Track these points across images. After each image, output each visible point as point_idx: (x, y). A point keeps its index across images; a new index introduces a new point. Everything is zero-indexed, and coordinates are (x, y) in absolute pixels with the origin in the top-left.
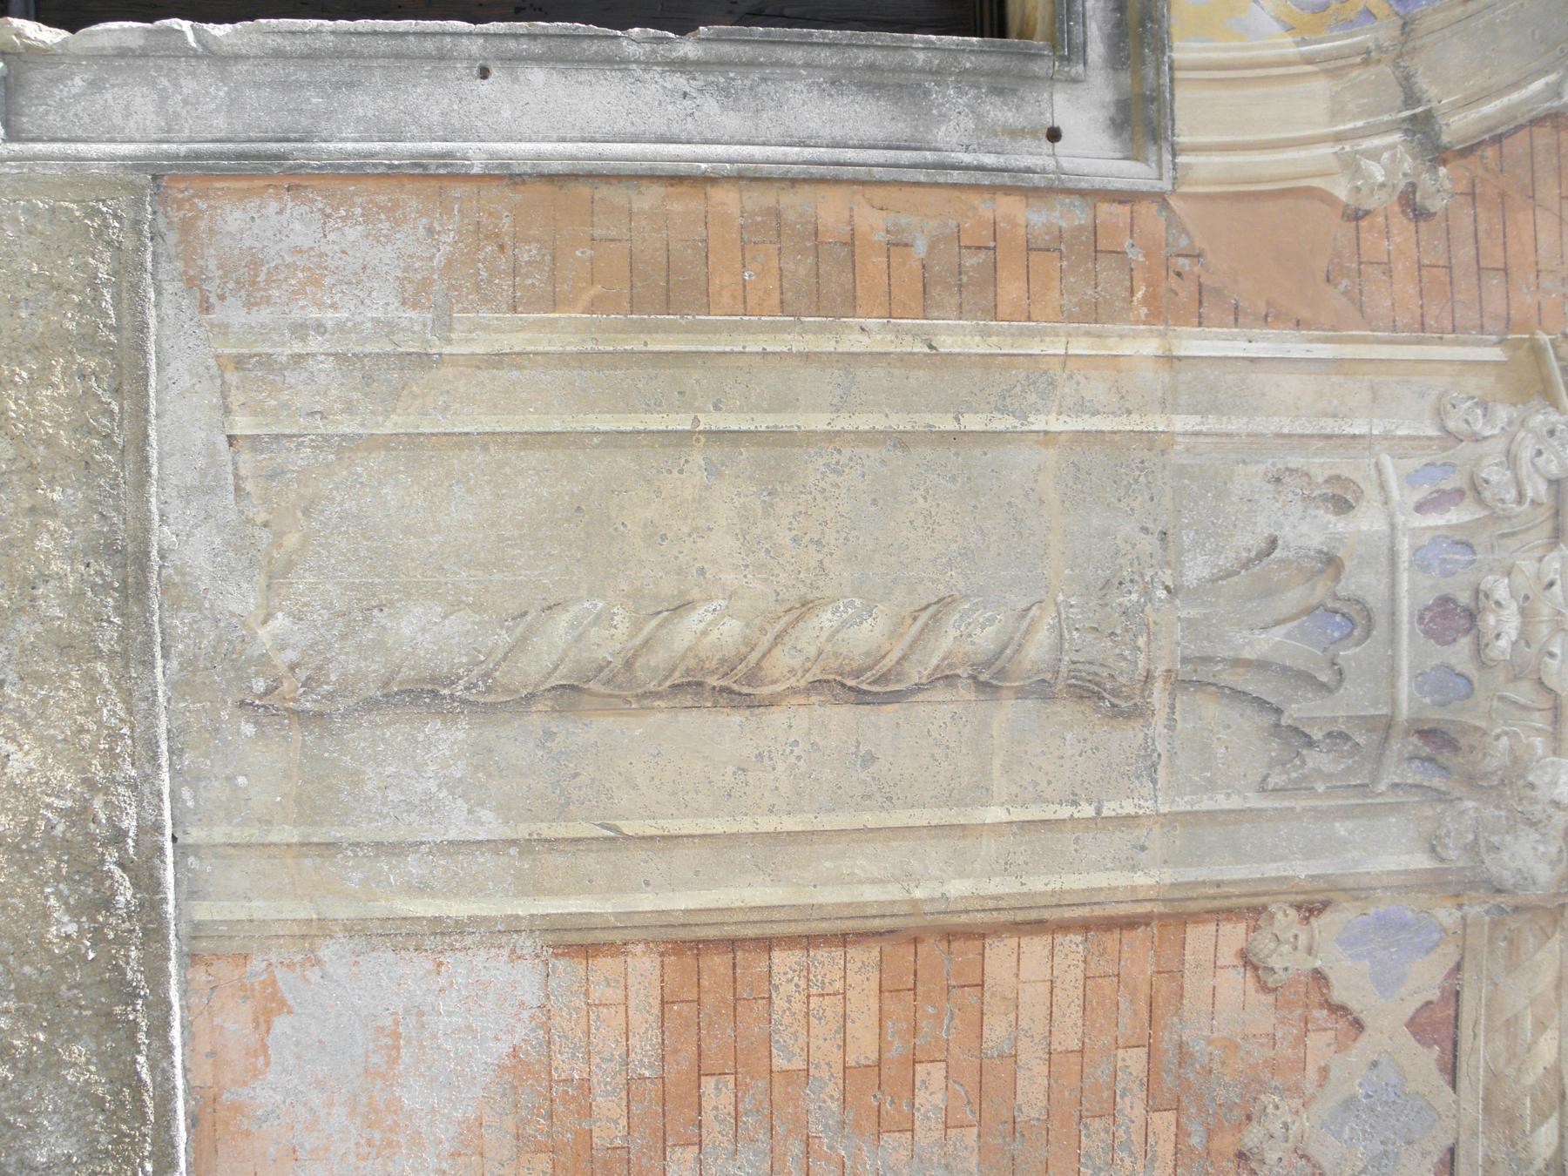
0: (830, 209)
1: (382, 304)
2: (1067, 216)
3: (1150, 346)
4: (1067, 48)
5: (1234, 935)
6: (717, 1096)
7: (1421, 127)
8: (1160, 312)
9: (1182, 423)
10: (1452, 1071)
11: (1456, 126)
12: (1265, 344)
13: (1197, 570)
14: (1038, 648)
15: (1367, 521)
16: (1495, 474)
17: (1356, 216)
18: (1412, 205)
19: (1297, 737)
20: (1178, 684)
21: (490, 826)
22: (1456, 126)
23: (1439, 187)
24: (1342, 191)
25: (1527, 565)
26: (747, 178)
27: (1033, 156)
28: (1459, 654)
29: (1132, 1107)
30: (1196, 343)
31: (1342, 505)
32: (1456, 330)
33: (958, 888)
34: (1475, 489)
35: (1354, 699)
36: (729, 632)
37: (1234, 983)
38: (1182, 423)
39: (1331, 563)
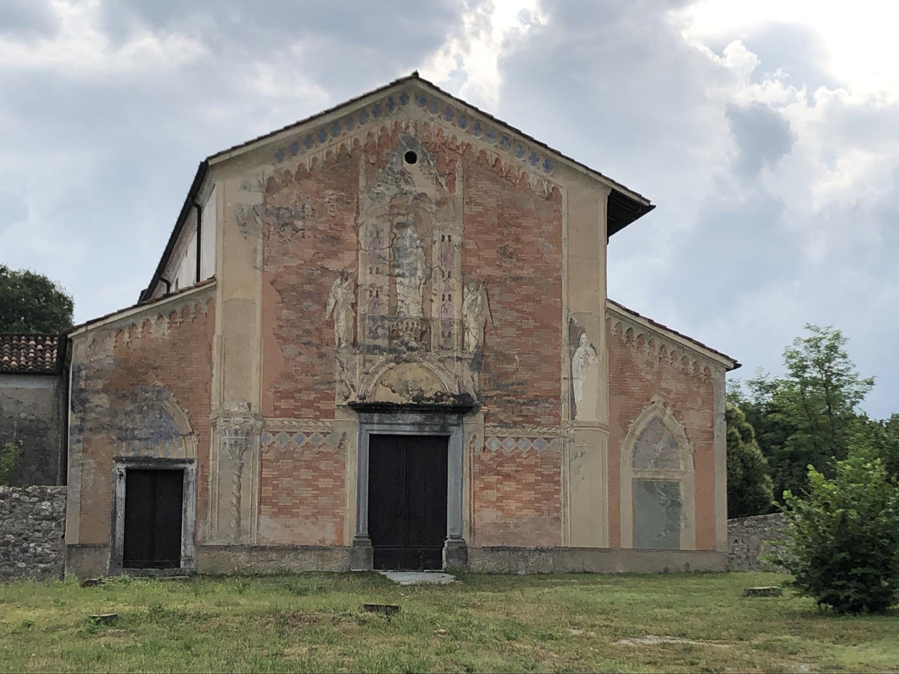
0: (199, 490)
1: (206, 526)
2: (200, 469)
3: (211, 462)
4: (185, 468)
5: (264, 454)
6: (274, 501)
7: (191, 434)
8: (208, 461)
9: (218, 459)
10: (278, 432)
11: (191, 430)
12: (211, 452)
13: (231, 458)
14: (237, 472)
15: (227, 441)
16: (223, 428)
17: (199, 442)
18: (198, 436)
19: (247, 448)
20: (241, 460)
21: (249, 519)
22: (191, 430)
23: (197, 432)
24: (197, 443)
25: (232, 425)
26: (197, 497)
27: (194, 472)
28: (239, 432)
29: (278, 464)
30: (211, 457)
31: (225, 443)
32: (210, 432)
33: (257, 479)
34: (224, 430)
35: (243, 442)
36: (235, 499)
37: (268, 454)
38: (218, 459)
39: (231, 445)
